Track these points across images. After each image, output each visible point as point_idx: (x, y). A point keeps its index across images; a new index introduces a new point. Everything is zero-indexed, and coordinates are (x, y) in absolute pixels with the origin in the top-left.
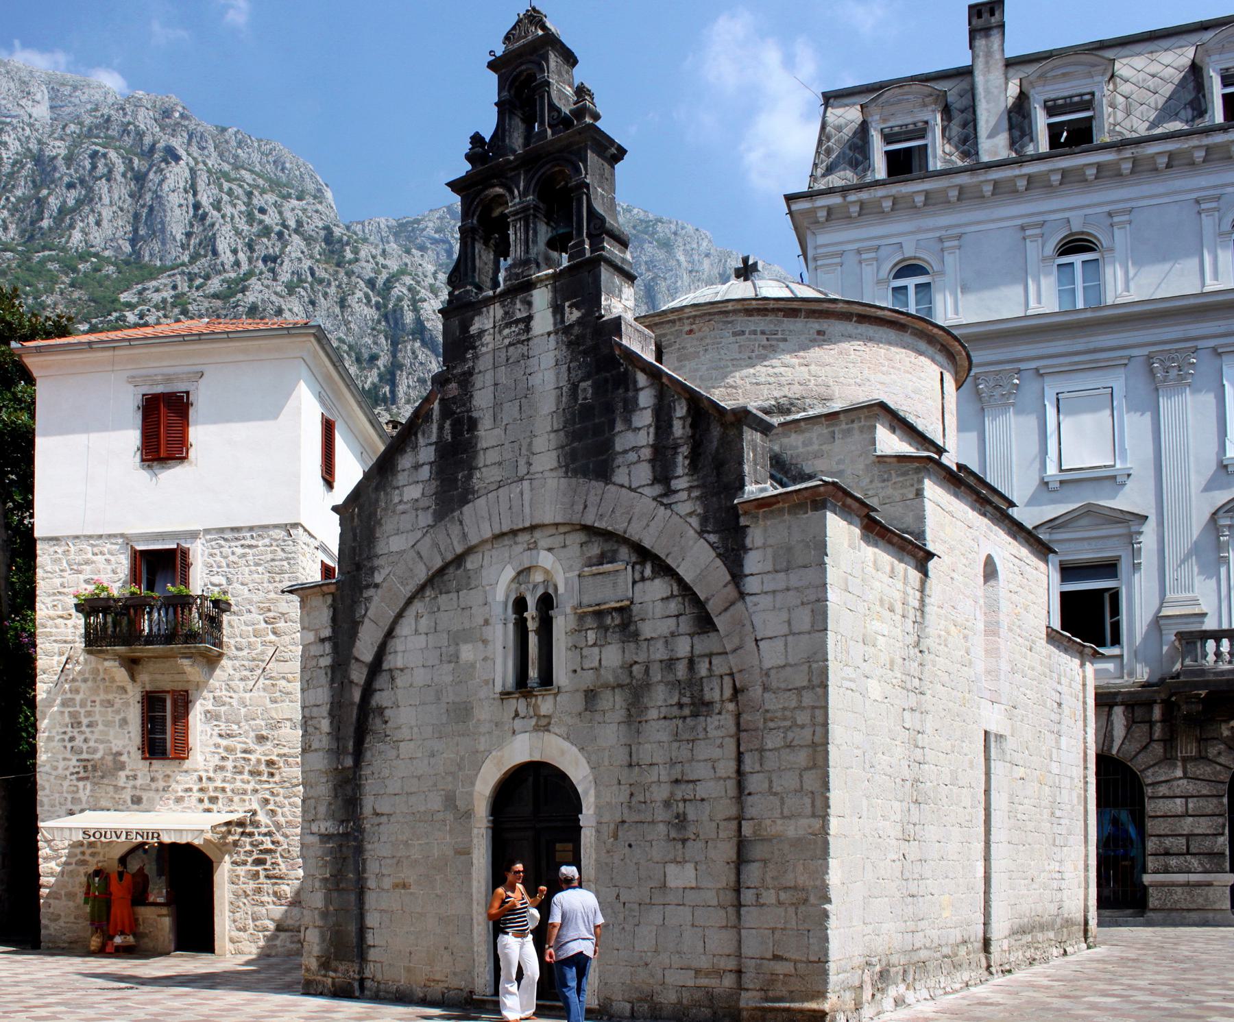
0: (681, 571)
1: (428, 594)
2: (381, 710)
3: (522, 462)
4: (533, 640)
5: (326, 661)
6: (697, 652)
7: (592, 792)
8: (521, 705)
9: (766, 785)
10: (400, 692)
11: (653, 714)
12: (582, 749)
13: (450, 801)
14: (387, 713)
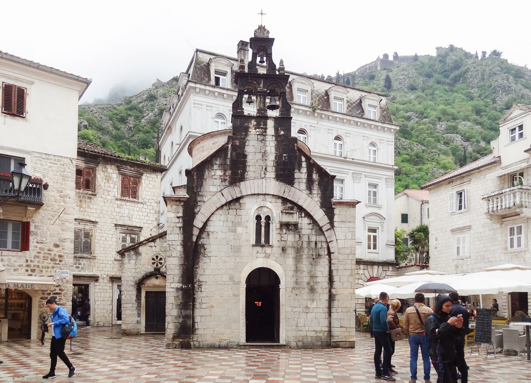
0: (314, 217)
1: (224, 208)
2: (203, 246)
3: (263, 173)
4: (263, 229)
5: (181, 225)
6: (317, 240)
7: (284, 278)
8: (259, 249)
9: (339, 279)
10: (211, 240)
11: (304, 257)
12: (281, 265)
13: (231, 278)
14: (206, 246)
